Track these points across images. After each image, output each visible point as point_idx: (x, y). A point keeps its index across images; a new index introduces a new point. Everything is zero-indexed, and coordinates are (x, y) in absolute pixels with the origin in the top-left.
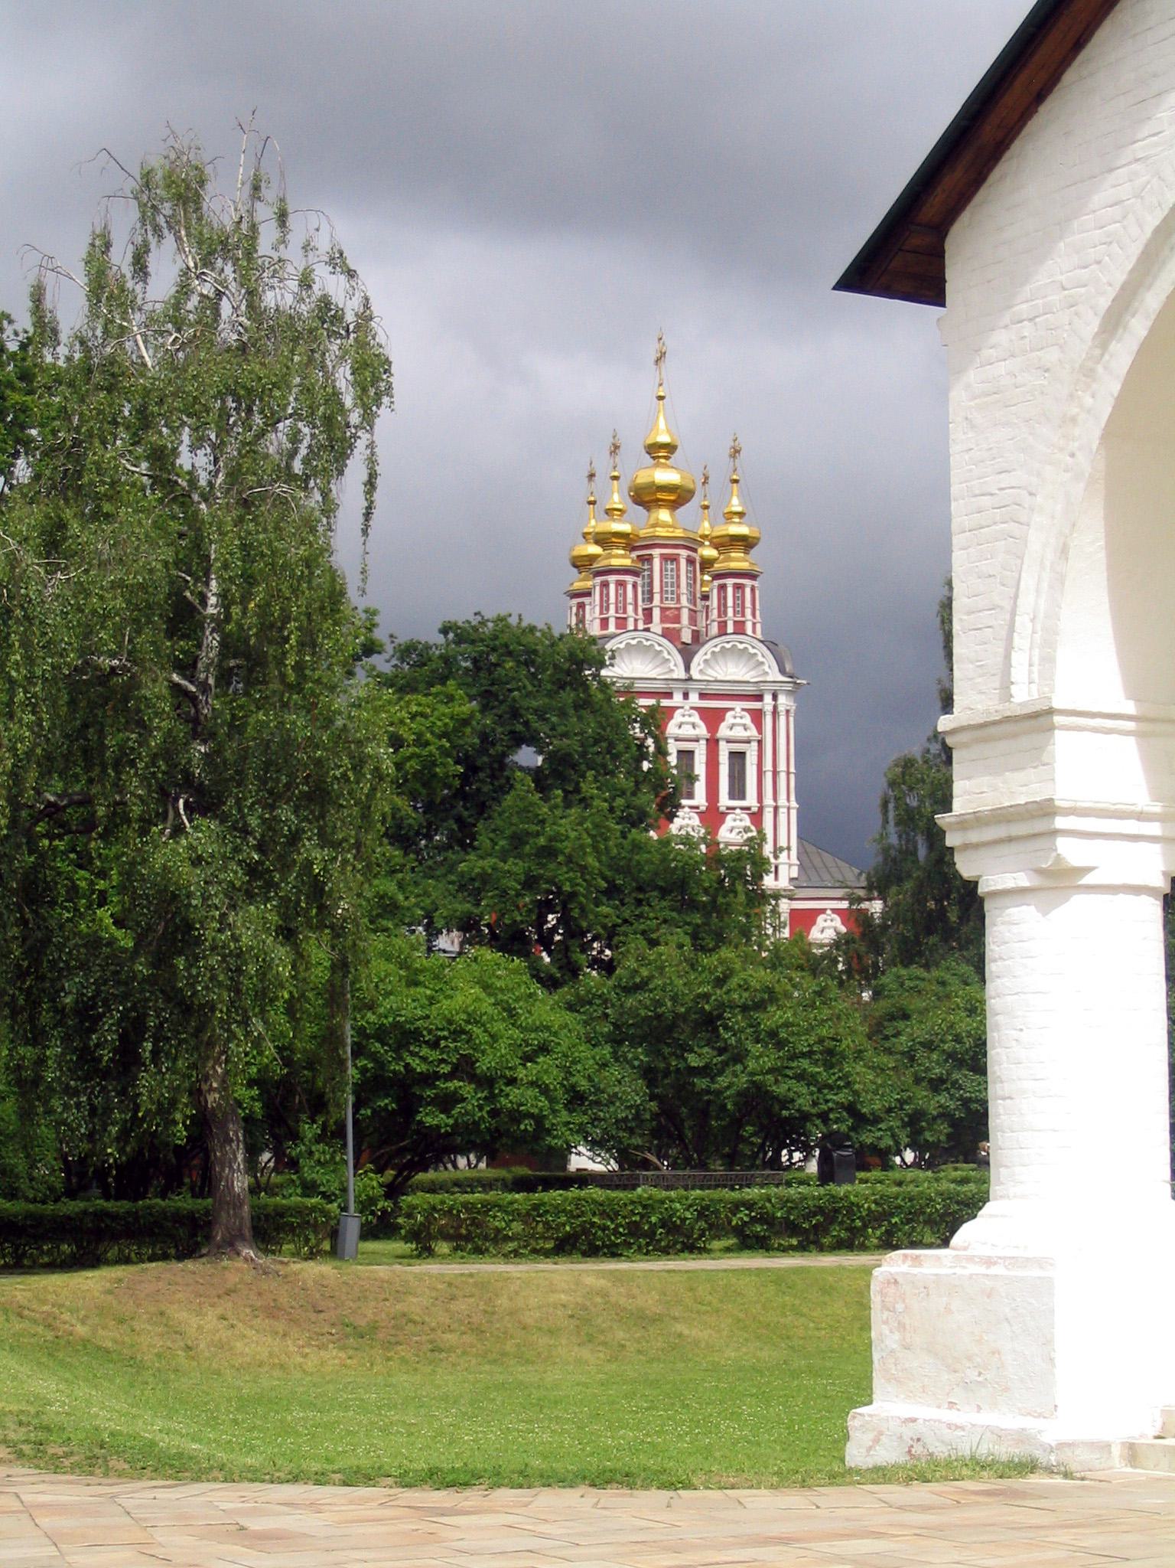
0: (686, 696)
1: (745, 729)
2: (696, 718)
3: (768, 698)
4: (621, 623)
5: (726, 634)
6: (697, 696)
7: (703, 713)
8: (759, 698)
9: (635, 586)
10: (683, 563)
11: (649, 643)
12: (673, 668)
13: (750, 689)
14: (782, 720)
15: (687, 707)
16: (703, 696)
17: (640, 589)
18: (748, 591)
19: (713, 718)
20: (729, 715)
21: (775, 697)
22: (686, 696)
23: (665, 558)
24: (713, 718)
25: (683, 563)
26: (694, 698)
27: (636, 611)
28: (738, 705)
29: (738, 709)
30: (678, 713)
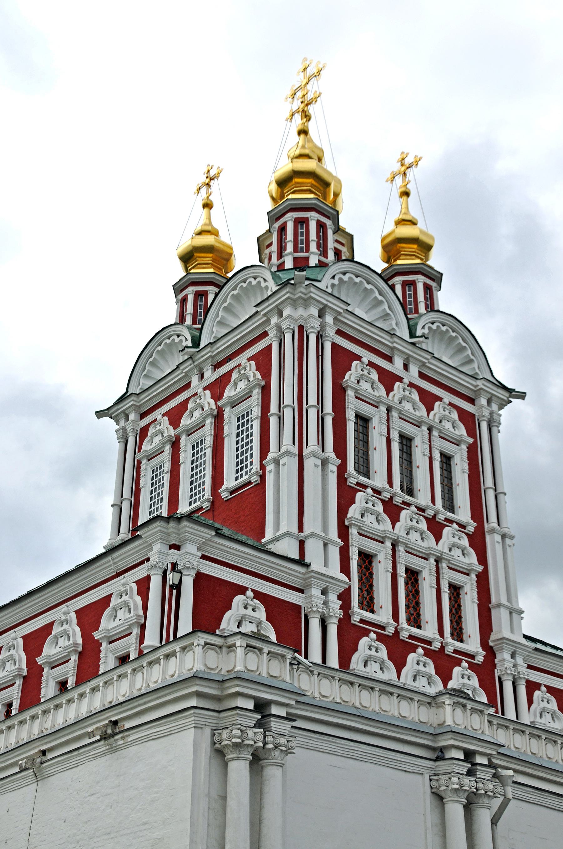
0: (406, 367)
3: (484, 402)
12: (394, 326)
22: (406, 367)
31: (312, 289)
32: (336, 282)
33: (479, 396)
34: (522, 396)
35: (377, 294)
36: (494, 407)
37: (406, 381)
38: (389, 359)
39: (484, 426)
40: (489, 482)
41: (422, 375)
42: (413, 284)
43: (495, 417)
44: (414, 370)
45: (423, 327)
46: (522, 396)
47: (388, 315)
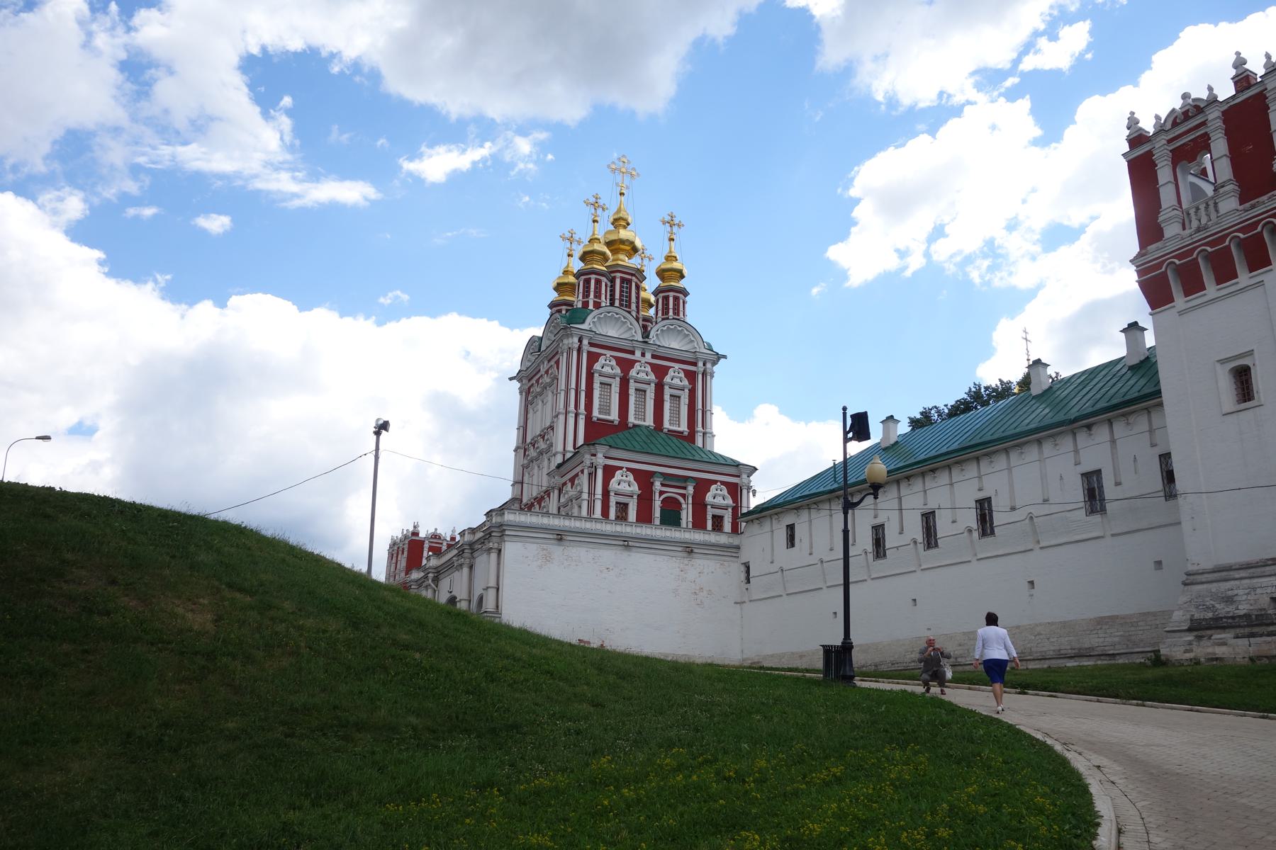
0: (643, 355)
1: (681, 381)
2: (648, 369)
4: (597, 305)
5: (668, 319)
6: (650, 356)
7: (654, 367)
8: (695, 364)
9: (606, 285)
10: (633, 285)
11: (617, 316)
12: (634, 334)
13: (689, 357)
14: (708, 377)
15: (643, 362)
16: (654, 357)
17: (608, 289)
18: (681, 301)
19: (660, 372)
20: (671, 372)
21: (704, 365)
22: (643, 355)
23: (623, 280)
24: (660, 372)
25: (633, 285)
26: (648, 356)
27: (606, 299)
28: (677, 366)
29: (677, 368)
30: (637, 366)
31: (572, 329)
32: (596, 320)
33: (698, 361)
34: (725, 357)
35: (623, 319)
36: (709, 365)
37: (643, 362)
38: (633, 353)
39: (700, 376)
40: (700, 406)
41: (654, 357)
42: (668, 297)
43: (708, 371)
44: (648, 356)
45: (657, 331)
46: (725, 357)
47: (631, 328)
